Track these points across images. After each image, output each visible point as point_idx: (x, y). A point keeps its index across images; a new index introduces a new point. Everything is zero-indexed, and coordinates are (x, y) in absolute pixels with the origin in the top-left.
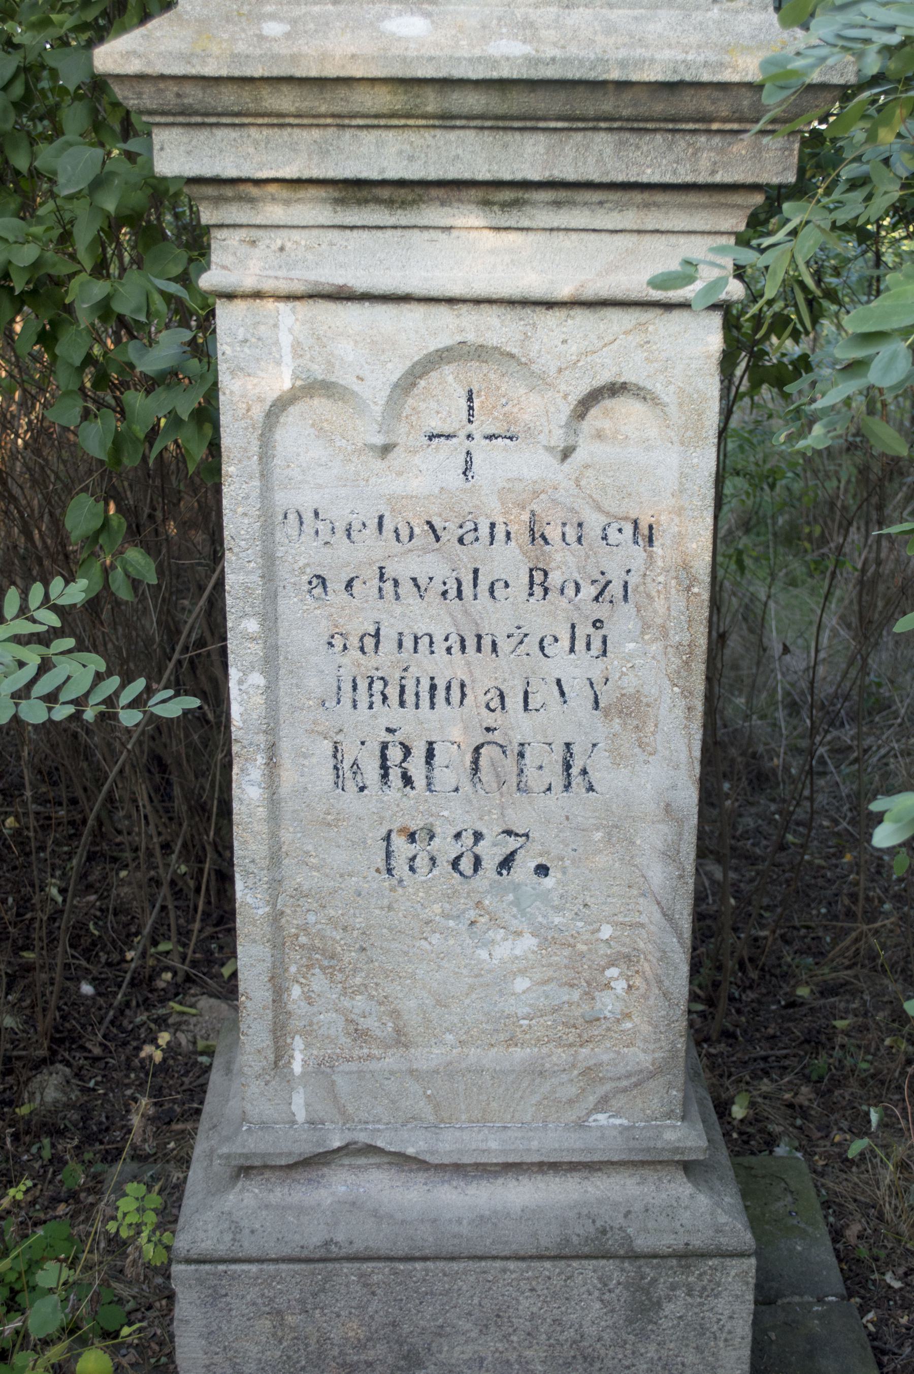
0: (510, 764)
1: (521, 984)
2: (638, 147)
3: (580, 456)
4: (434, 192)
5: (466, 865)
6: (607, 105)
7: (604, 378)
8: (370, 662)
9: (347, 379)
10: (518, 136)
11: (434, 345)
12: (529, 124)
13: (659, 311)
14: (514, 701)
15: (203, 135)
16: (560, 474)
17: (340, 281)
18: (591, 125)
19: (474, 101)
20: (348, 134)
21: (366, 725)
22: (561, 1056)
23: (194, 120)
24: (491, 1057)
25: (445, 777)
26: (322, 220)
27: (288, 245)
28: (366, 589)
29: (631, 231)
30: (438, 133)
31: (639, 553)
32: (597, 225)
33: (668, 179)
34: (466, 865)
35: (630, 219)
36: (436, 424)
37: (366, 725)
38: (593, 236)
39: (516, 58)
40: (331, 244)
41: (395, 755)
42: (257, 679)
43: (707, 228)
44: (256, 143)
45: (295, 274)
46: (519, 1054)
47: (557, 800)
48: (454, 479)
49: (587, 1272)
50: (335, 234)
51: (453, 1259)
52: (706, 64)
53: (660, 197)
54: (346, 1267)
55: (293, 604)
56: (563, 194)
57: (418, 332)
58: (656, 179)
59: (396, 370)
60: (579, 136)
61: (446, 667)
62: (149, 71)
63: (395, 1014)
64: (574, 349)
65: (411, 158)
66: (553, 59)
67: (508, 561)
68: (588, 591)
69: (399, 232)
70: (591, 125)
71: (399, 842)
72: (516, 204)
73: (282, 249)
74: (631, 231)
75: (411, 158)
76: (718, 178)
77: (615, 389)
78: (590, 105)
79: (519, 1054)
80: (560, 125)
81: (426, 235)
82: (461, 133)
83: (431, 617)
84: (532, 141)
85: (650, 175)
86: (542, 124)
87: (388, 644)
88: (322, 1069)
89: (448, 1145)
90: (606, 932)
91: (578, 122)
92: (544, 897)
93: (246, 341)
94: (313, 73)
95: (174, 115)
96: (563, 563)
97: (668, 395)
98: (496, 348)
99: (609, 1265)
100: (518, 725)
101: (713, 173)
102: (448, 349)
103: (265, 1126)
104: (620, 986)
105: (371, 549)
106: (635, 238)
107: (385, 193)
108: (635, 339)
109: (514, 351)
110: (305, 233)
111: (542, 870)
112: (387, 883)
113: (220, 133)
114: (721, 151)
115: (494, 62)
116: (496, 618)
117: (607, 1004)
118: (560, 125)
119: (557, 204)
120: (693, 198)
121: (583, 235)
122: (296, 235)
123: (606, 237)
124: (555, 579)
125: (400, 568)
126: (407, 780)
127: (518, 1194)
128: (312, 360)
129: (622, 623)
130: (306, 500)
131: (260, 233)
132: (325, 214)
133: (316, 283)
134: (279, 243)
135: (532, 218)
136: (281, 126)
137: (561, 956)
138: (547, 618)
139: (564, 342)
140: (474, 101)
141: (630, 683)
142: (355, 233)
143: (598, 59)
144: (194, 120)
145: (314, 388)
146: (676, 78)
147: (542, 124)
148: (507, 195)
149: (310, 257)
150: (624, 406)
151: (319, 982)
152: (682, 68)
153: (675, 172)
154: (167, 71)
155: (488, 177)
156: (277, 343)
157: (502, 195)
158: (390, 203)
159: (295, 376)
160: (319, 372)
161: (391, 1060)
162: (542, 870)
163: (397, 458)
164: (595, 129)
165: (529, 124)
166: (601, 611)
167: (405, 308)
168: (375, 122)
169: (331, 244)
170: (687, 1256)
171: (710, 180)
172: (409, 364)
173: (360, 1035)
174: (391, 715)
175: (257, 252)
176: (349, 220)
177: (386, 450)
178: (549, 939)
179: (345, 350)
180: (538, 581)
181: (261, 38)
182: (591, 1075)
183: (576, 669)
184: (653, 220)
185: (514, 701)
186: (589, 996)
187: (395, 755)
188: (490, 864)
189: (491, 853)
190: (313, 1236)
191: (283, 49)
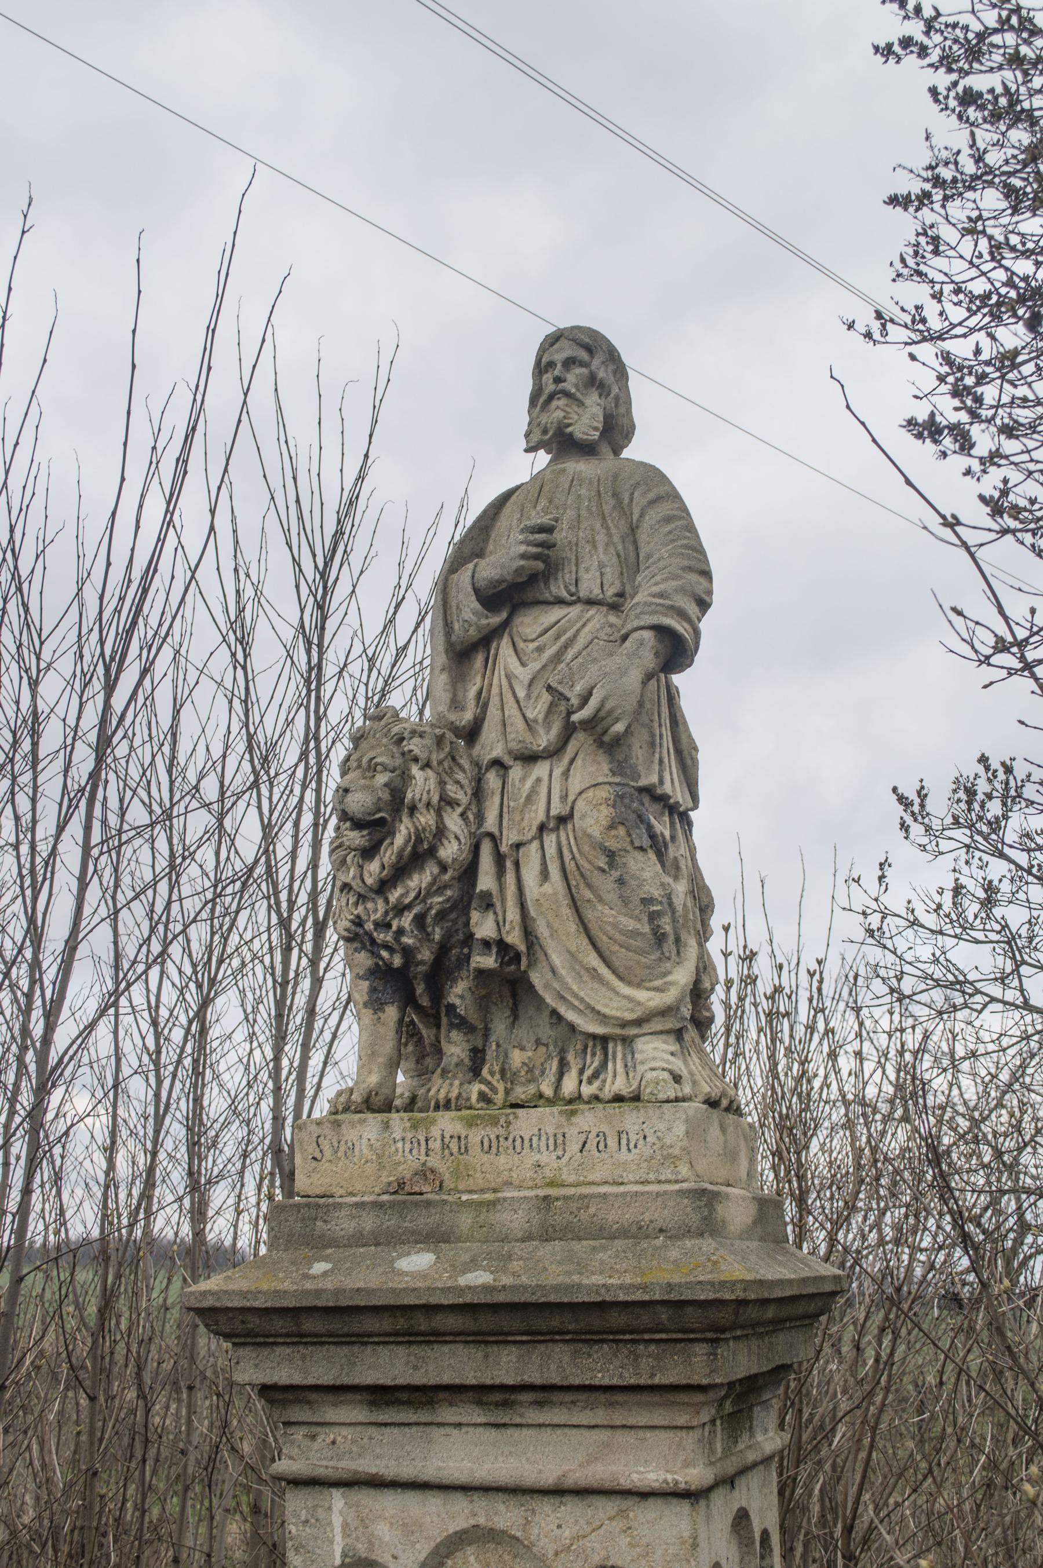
2: (590, 1355)
4: (441, 1395)
6: (556, 1323)
10: (495, 1348)
12: (500, 1338)
13: (637, 1499)
15: (265, 1352)
17: (373, 1470)
18: (548, 1337)
19: (452, 1322)
20: (369, 1349)
23: (258, 1340)
26: (361, 1418)
27: (339, 1439)
29: (604, 1427)
30: (435, 1346)
32: (574, 1421)
33: (615, 1381)
35: (599, 1416)
38: (574, 1431)
39: (477, 1287)
40: (371, 1438)
43: (666, 1423)
44: (303, 1358)
45: (342, 1464)
50: (373, 1431)
52: (621, 1287)
53: (620, 1397)
56: (540, 1396)
58: (606, 1382)
60: (542, 1347)
62: (218, 1304)
64: (567, 1533)
65: (416, 1368)
66: (504, 1287)
69: (421, 1428)
70: (548, 1337)
72: (505, 1404)
73: (334, 1443)
74: (604, 1427)
75: (416, 1368)
76: (656, 1380)
78: (540, 1323)
80: (525, 1338)
81: (443, 1430)
82: (453, 1346)
84: (506, 1352)
85: (601, 1378)
86: (510, 1338)
93: (307, 1521)
94: (331, 1304)
95: (245, 1336)
98: (503, 1532)
101: (653, 1376)
102: (465, 1532)
106: (609, 1433)
107: (404, 1396)
108: (617, 1526)
109: (519, 1534)
110: (351, 1430)
113: (279, 1350)
114: (658, 1358)
115: (461, 1290)
118: (525, 1338)
119: (540, 1404)
120: (646, 1397)
121: (566, 1430)
122: (345, 1431)
123: (586, 1433)
128: (357, 1539)
131: (318, 1429)
132: (359, 1413)
133: (356, 1472)
134: (332, 1436)
135: (521, 1416)
136: (322, 1344)
139: (559, 1527)
140: (452, 1322)
142: (388, 1430)
143: (538, 1286)
144: (258, 1340)
146: (599, 1299)
147: (510, 1338)
148: (498, 1397)
149: (355, 1449)
152: (603, 1291)
153: (621, 1376)
154: (230, 1305)
155: (474, 1382)
156: (330, 1524)
157: (496, 1398)
158: (409, 1403)
159: (344, 1555)
164: (553, 1341)
165: (500, 1338)
167: (429, 1494)
168: (387, 1339)
169: (371, 1438)
171: (650, 1382)
172: (433, 1544)
175: (316, 1445)
176: (382, 1418)
179: (383, 1530)
181: (306, 1276)
184: (619, 1418)
191: (329, 1284)
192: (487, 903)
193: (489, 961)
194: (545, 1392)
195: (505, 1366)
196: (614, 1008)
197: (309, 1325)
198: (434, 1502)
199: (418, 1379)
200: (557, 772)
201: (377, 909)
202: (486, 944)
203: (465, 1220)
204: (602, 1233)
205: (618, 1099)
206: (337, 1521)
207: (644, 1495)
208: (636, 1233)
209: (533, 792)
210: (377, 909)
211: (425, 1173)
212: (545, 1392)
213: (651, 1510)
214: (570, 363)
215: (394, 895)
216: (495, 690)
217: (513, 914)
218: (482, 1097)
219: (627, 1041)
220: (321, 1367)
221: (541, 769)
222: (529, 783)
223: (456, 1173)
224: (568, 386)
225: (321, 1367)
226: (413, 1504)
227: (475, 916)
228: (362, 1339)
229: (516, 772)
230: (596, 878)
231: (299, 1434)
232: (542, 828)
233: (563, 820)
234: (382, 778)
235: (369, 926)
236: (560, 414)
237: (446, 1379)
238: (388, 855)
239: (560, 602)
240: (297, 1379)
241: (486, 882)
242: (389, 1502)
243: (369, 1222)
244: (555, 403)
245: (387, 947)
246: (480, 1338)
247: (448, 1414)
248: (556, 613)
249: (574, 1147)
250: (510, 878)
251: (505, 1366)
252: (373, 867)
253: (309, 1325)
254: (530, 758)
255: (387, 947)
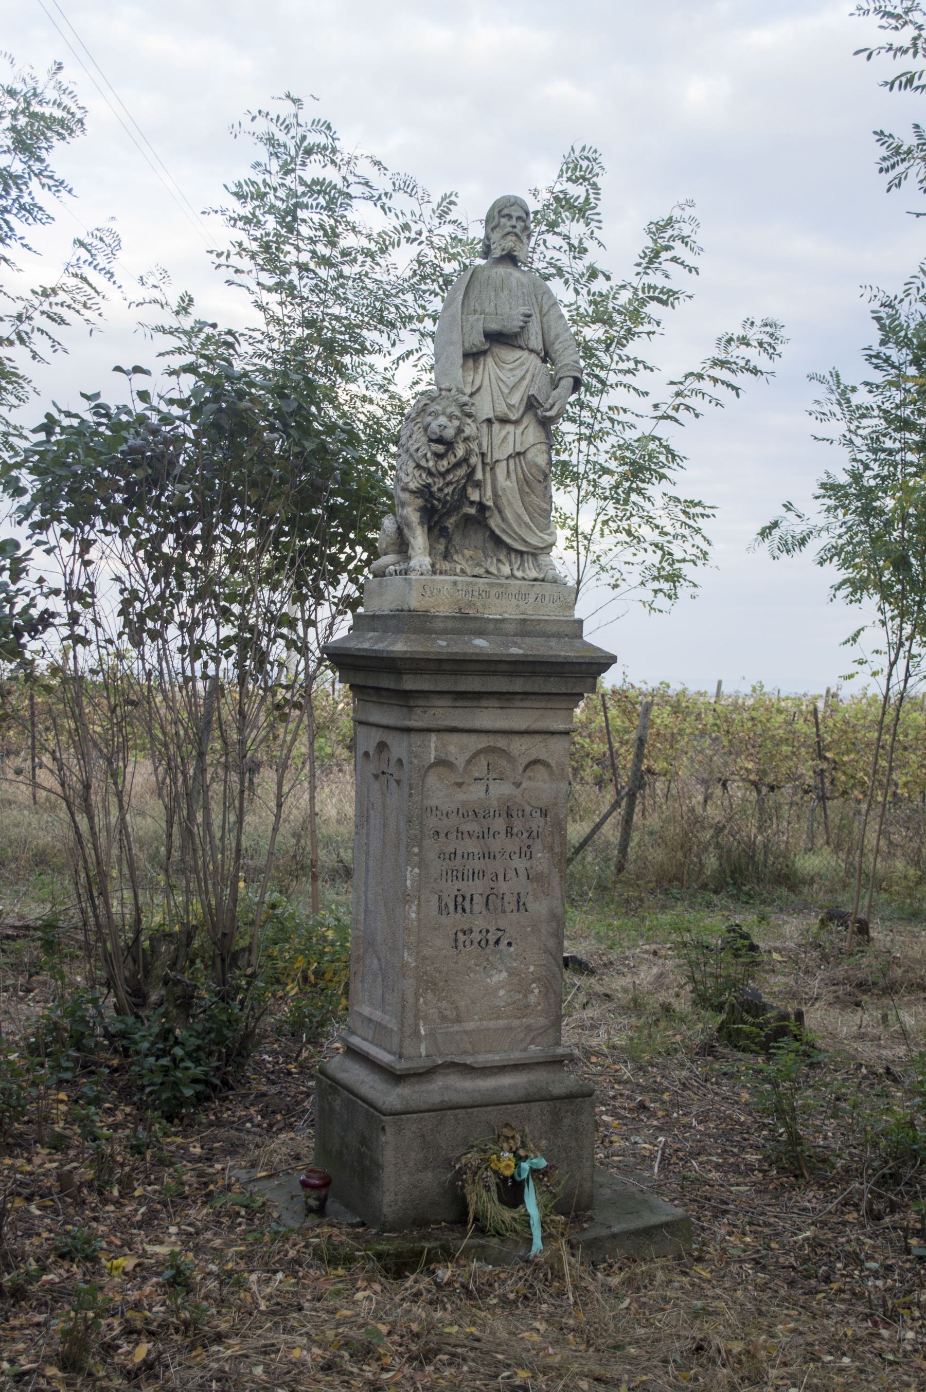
0: (499, 902)
1: (502, 993)
3: (523, 786)
5: (483, 943)
7: (534, 757)
8: (452, 864)
9: (452, 759)
11: (480, 746)
14: (501, 877)
16: (517, 792)
19: (505, 667)
21: (451, 888)
22: (516, 1022)
24: (492, 1024)
25: (476, 908)
28: (453, 836)
31: (542, 820)
34: (483, 943)
35: (543, 705)
36: (477, 775)
37: (451, 888)
41: (460, 899)
42: (417, 870)
46: (502, 1023)
47: (515, 916)
48: (482, 794)
49: (536, 1107)
51: (487, 1105)
54: (449, 1112)
55: (428, 842)
57: (476, 743)
59: (467, 756)
61: (477, 865)
63: (457, 1008)
67: (499, 824)
68: (526, 834)
71: (460, 935)
77: (536, 762)
79: (502, 1023)
83: (472, 846)
85: (554, 690)
87: (459, 857)
88: (432, 1034)
89: (482, 1059)
90: (532, 969)
91: (534, 674)
92: (510, 955)
96: (518, 825)
97: (553, 764)
99: (544, 1104)
100: (503, 886)
103: (410, 1058)
104: (536, 991)
105: (454, 820)
111: (510, 944)
112: (454, 952)
116: (496, 845)
117: (532, 999)
124: (515, 830)
125: (465, 828)
126: (464, 910)
127: (506, 1081)
129: (538, 846)
130: (434, 802)
137: (515, 980)
138: (511, 845)
141: (540, 869)
145: (442, 763)
150: (540, 768)
151: (430, 996)
157: (505, 698)
160: (443, 756)
161: (456, 1028)
162: (510, 944)
163: (465, 787)
166: (530, 842)
170: (571, 1097)
173: (444, 1018)
174: (459, 884)
177: (460, 785)
178: (512, 973)
179: (452, 749)
180: (509, 832)
182: (528, 1028)
183: (520, 864)
185: (501, 877)
186: (525, 996)
187: (460, 899)
188: (491, 943)
189: (492, 938)
190: (436, 1099)
192: (478, 485)
193: (472, 511)
194: (526, 694)
195: (518, 685)
196: (534, 541)
197: (446, 667)
198: (473, 738)
199: (483, 689)
200: (519, 432)
201: (440, 483)
202: (472, 503)
203: (491, 626)
204: (547, 635)
205: (535, 580)
206: (433, 745)
207: (553, 733)
208: (559, 636)
209: (505, 438)
210: (440, 483)
211: (471, 605)
212: (526, 694)
213: (557, 737)
214: (519, 218)
215: (450, 477)
216: (486, 382)
217: (489, 493)
218: (462, 571)
219: (534, 555)
220: (444, 684)
221: (510, 428)
222: (503, 433)
223: (484, 606)
224: (517, 231)
225: (444, 684)
226: (465, 738)
227: (470, 490)
228: (462, 673)
229: (496, 426)
230: (535, 484)
231: (419, 711)
232: (510, 456)
233: (519, 454)
234: (456, 423)
235: (435, 489)
236: (511, 244)
237: (495, 689)
238: (453, 460)
239: (521, 348)
240: (432, 688)
241: (479, 475)
242: (455, 738)
243: (450, 624)
244: (509, 238)
245: (439, 500)
246: (511, 674)
247: (484, 703)
248: (518, 353)
249: (531, 600)
250: (488, 475)
251: (518, 685)
252: (445, 462)
253: (446, 667)
254: (504, 421)
255: (439, 500)
